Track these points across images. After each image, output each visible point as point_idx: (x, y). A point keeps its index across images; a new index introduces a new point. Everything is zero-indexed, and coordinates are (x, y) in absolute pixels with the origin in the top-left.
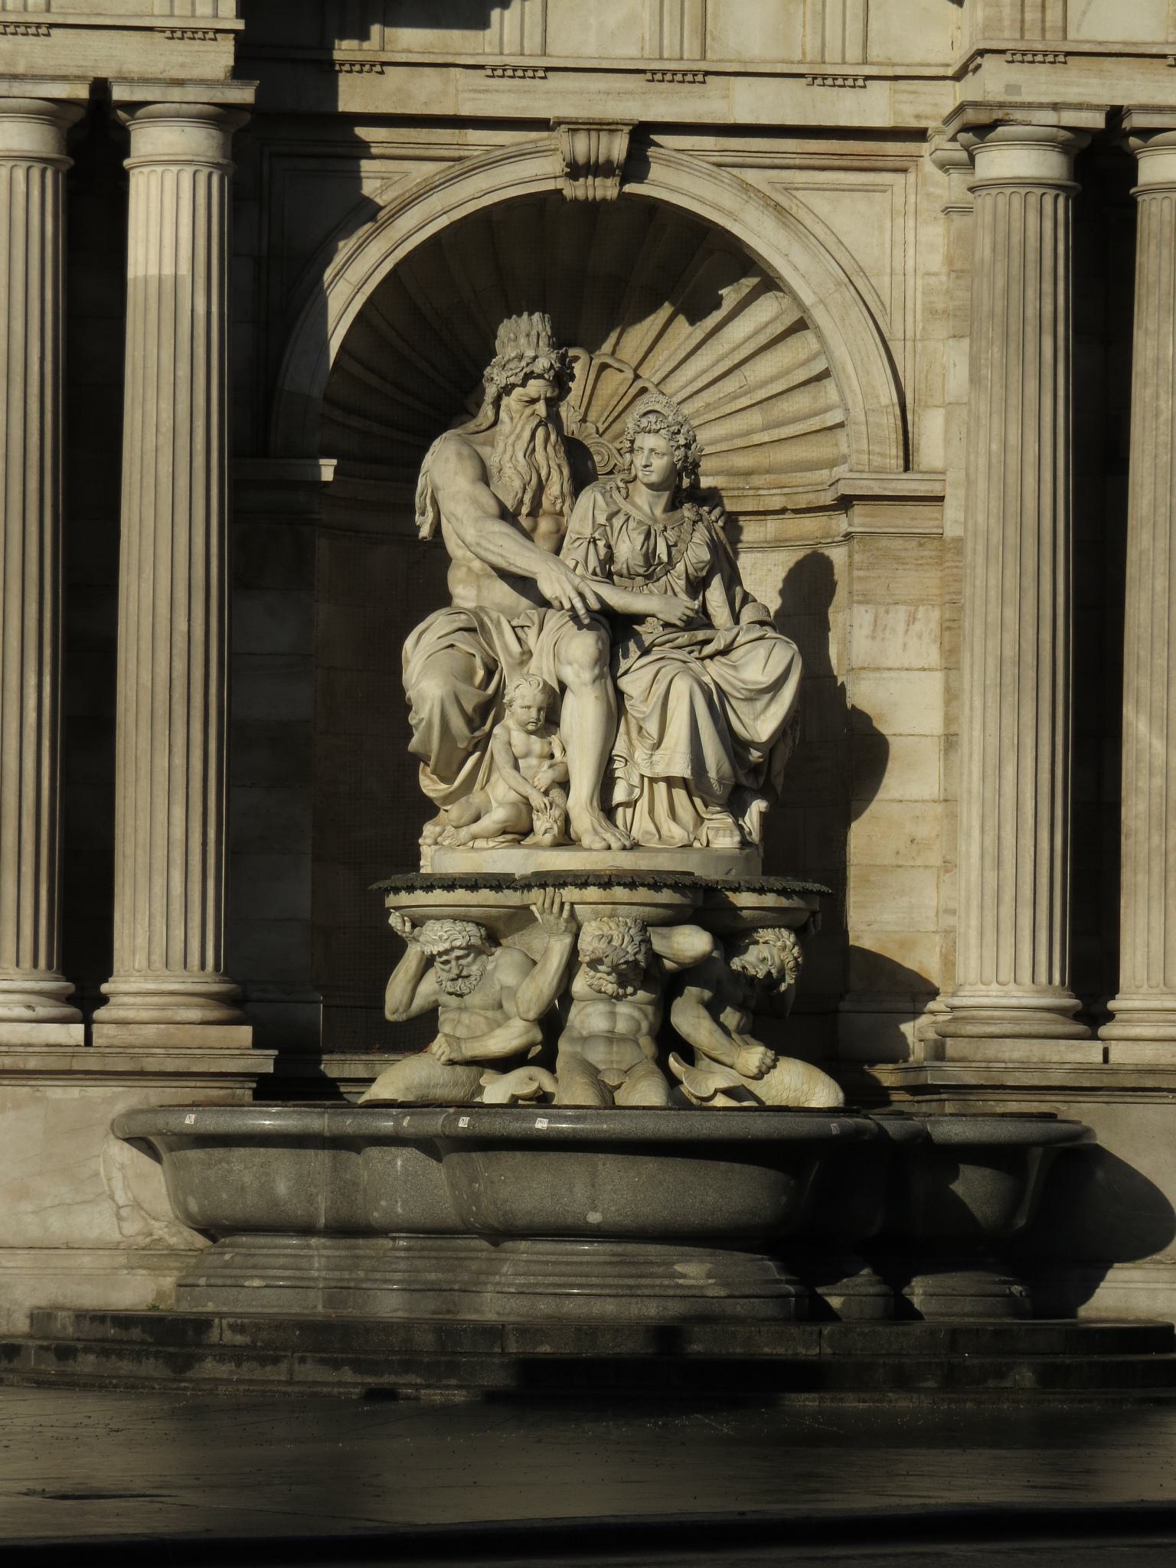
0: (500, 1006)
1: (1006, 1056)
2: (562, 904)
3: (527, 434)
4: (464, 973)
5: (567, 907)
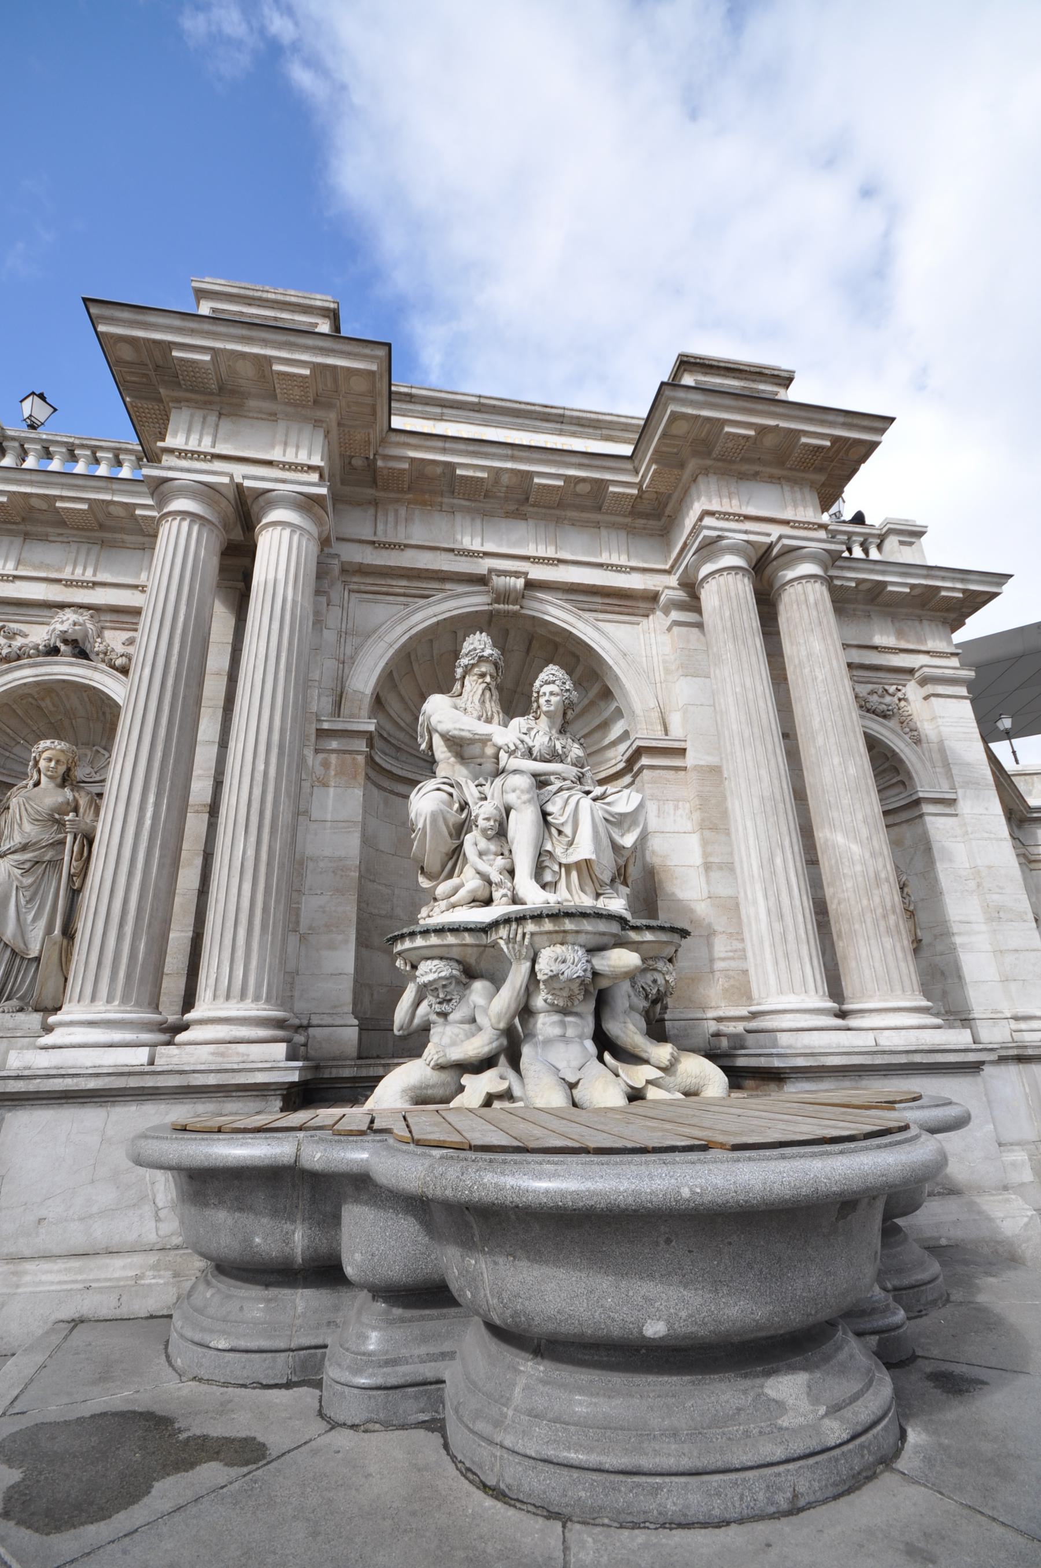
0: (474, 1020)
1: (816, 1043)
2: (524, 934)
3: (480, 692)
4: (448, 997)
5: (527, 936)
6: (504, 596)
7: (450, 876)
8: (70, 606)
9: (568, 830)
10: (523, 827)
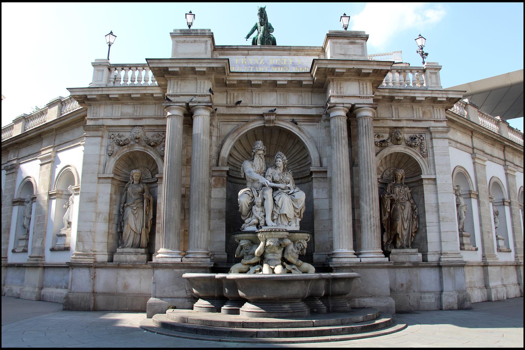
6: (269, 121)
7: (249, 217)
8: (136, 126)
9: (280, 206)
10: (269, 204)
